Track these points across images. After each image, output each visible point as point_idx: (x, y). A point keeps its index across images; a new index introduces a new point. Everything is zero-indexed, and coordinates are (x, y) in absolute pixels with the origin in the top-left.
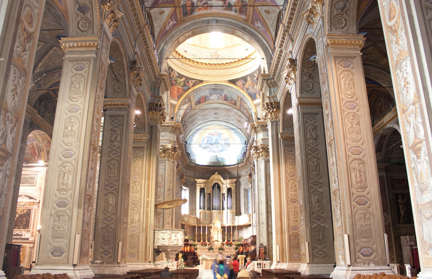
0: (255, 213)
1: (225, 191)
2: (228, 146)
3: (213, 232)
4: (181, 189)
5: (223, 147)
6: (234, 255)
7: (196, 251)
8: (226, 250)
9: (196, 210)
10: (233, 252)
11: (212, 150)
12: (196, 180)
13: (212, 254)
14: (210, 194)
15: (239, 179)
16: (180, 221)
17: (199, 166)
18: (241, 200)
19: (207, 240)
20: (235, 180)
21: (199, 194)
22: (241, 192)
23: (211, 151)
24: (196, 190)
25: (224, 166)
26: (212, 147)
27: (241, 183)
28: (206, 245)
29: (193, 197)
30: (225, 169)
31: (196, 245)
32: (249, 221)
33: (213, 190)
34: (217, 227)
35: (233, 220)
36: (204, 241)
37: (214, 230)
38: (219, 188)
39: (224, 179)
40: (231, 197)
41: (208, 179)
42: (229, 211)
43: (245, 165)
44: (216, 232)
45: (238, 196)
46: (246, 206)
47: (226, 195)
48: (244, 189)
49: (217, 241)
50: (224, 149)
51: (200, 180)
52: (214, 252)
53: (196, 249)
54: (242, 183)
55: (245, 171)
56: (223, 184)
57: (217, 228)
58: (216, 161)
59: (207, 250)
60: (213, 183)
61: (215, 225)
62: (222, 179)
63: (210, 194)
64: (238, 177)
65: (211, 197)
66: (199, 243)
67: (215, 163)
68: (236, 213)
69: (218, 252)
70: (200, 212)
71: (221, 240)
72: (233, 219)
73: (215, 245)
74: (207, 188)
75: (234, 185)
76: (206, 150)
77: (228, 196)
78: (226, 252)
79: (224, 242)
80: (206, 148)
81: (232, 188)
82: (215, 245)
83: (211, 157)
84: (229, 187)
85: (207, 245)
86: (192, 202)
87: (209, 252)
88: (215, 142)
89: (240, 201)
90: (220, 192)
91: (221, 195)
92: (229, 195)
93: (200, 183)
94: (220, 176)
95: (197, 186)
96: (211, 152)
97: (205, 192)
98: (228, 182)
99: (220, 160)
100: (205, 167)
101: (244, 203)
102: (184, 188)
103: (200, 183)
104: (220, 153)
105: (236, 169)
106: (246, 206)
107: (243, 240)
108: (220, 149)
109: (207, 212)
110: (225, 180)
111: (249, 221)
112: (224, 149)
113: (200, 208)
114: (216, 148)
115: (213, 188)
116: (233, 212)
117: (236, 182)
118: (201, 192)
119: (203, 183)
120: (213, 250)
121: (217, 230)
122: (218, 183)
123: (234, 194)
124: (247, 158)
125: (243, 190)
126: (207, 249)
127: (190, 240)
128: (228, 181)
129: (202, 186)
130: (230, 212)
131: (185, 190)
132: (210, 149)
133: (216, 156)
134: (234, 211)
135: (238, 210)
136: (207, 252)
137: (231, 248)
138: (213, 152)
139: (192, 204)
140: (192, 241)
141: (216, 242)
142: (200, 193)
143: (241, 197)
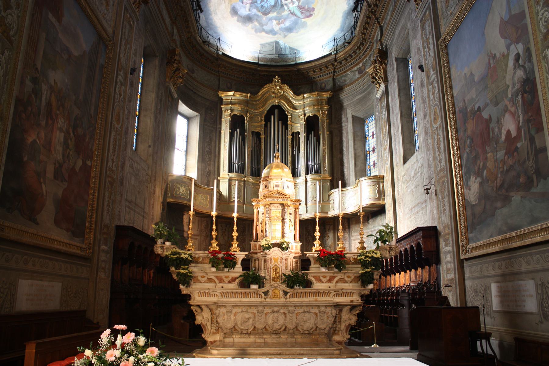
0: (416, 159)
1: (299, 126)
2: (308, 14)
3: (262, 210)
4: (176, 112)
5: (293, 18)
6: (353, 307)
7: (184, 290)
8: (317, 285)
9: (219, 175)
10: (351, 294)
11: (266, 28)
12: (220, 93)
13: (256, 300)
14: (258, 135)
15: (339, 95)
16: (159, 192)
17: (230, 60)
18: (345, 149)
19: (235, 244)
20: (326, 95)
21: (228, 131)
22: (344, 128)
23: (263, 30)
24: (221, 124)
25: (297, 64)
26: (264, 19)
27: (345, 104)
28: (230, 262)
29: (211, 139)
30: (299, 70)
31: (186, 262)
32: (379, 199)
33: (266, 126)
34: (279, 189)
35: (325, 201)
36: (226, 245)
37: (268, 201)
38: (284, 118)
39: (297, 93)
40: (318, 140)
41: (254, 93)
42: (309, 177)
43: (362, 44)
44: (276, 211)
45: (336, 140)
46: (359, 163)
47: (302, 137)
48: (353, 117)
49: (279, 245)
50: (296, 23)
51: (232, 93)
52: (266, 293)
53: (187, 279)
54: (345, 104)
55: (355, 68)
56: (295, 108)
57: (282, 195)
58: (276, 56)
59: (234, 286)
60: (268, 107)
61: (273, 183)
62: (290, 94)
63: (258, 135)
64: (337, 90)
65: (263, 141)
66: (201, 254)
67: (272, 60)
68: (331, 181)
69: (286, 293)
70: (230, 180)
71: (295, 247)
72: (322, 200)
73: (271, 265)
74: (251, 118)
75: (326, 107)
76: (250, 25)
77: (307, 138)
78: (318, 293)
79: (308, 254)
80: (248, 19)
81: (320, 117)
82: (268, 265)
83: (262, 45)
84: (310, 114)
85: (235, 264)
86: (209, 153)
87: (246, 295)
88: (273, 3)
89: (341, 152)
90: (287, 128)
91: (290, 137)
92: (312, 136)
93: (231, 103)
94: (286, 87)
95: (223, 109)
96: (264, 34)
97: (246, 127)
98: (307, 101)
99: (288, 52)
100: (246, 65)
101: (355, 154)
102: (183, 108)
103: (231, 103)
104: (285, 36)
105: (330, 67)
106: (359, 163)
107: (393, 243)
108: (287, 24)
109: (250, 179)
110: (300, 97)
111: (379, 199)
112: (296, 23)
113: (230, 170)
114: (274, 22)
115: (267, 119)
116: (323, 181)
117: (329, 101)
118: (233, 128)
119: (239, 102)
120: (261, 286)
121: (280, 201)
122: (282, 105)
123: (327, 133)
124: (369, 5)
125: (350, 120)
126: (234, 280)
127: (159, 241)
128: (308, 98)
129: (238, 110)
130: (315, 180)
131: (188, 118)
132: (261, 25)
133: (277, 43)
134: (328, 177)
135: (335, 175)
136: (235, 294)
137: (339, 276)
138: (267, 33)
139: (207, 159)
140: (168, 243)
141: (275, 252)
142: (231, 129)
143: (344, 139)
